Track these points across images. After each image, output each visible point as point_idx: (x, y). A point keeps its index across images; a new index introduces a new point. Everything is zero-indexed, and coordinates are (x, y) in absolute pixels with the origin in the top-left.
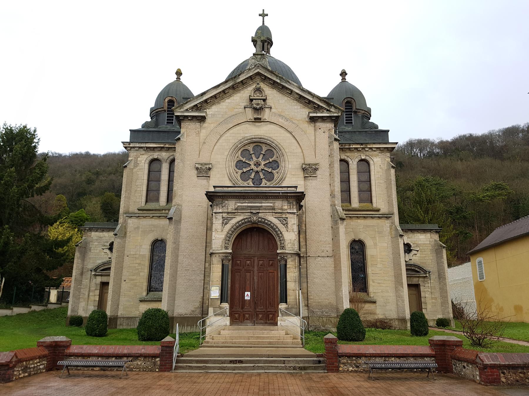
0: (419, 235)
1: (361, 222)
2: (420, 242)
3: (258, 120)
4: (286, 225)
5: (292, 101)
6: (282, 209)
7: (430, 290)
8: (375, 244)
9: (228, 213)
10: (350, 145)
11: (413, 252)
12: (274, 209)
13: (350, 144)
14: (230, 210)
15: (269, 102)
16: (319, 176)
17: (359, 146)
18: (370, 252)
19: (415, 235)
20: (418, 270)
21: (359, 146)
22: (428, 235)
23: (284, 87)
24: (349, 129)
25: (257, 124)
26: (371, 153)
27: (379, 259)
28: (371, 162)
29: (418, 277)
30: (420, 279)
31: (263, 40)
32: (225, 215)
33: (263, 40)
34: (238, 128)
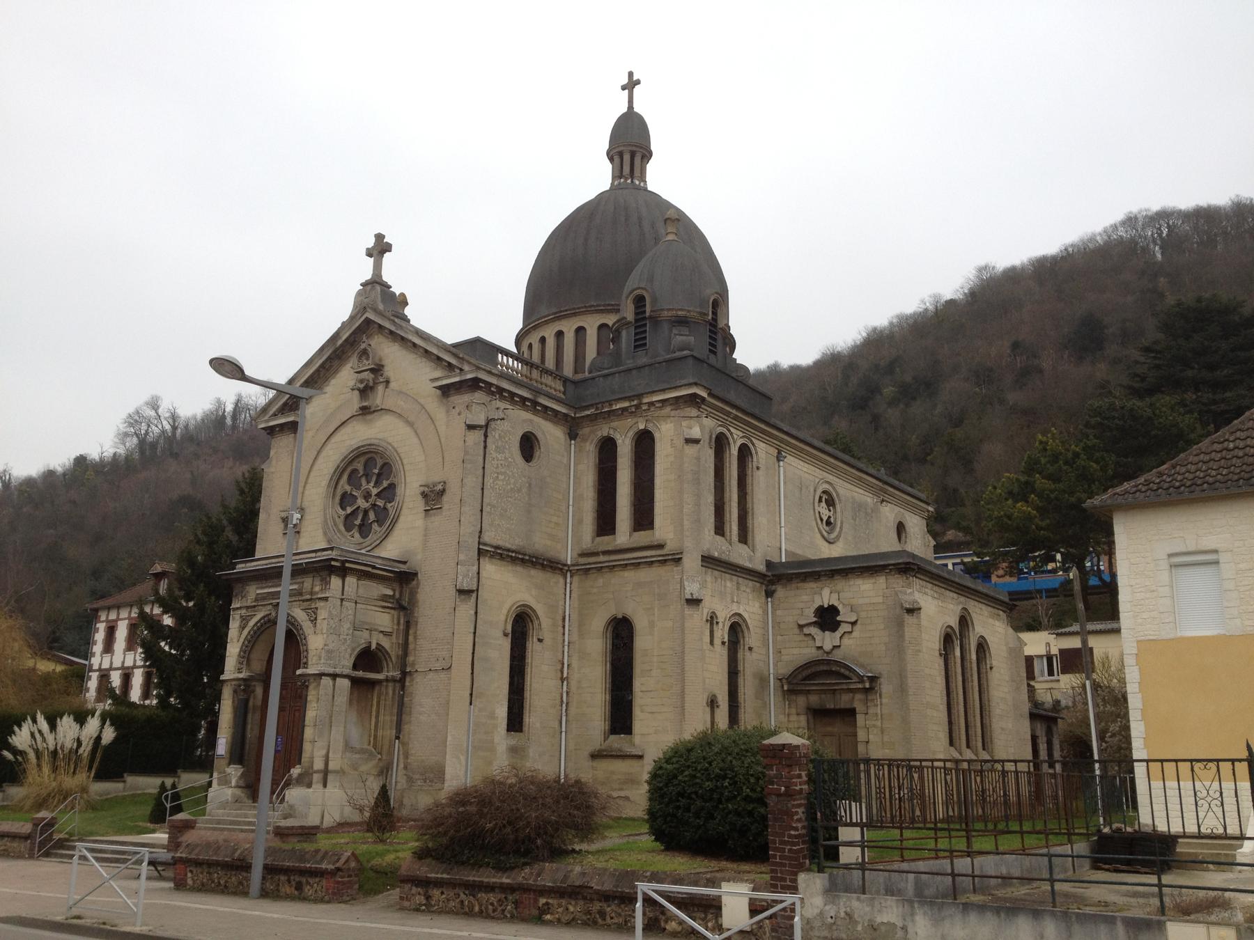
0: (859, 581)
1: (629, 574)
2: (861, 601)
3: (365, 411)
4: (314, 621)
5: (419, 360)
6: (312, 593)
7: (879, 723)
8: (652, 625)
9: (247, 608)
10: (611, 405)
11: (845, 628)
12: (301, 594)
13: (610, 403)
14: (249, 604)
15: (389, 371)
16: (446, 507)
17: (626, 404)
18: (642, 643)
19: (852, 582)
20: (847, 673)
21: (626, 404)
22: (881, 581)
23: (403, 338)
24: (643, 360)
25: (369, 417)
26: (654, 412)
27: (655, 659)
28: (657, 435)
29: (851, 691)
30: (858, 696)
31: (630, 145)
32: (243, 611)
33: (630, 145)
34: (343, 431)
